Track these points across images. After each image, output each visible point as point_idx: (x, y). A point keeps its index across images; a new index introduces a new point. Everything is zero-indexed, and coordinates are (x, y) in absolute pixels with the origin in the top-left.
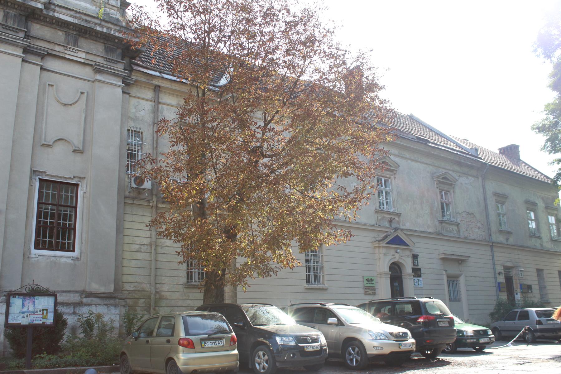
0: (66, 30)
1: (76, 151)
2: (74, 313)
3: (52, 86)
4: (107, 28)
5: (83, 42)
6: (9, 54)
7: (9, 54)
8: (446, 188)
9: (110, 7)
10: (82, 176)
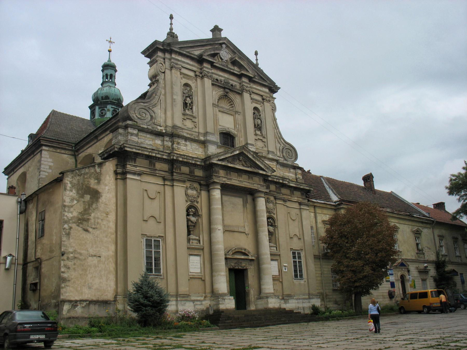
2: (309, 302)
8: (418, 236)
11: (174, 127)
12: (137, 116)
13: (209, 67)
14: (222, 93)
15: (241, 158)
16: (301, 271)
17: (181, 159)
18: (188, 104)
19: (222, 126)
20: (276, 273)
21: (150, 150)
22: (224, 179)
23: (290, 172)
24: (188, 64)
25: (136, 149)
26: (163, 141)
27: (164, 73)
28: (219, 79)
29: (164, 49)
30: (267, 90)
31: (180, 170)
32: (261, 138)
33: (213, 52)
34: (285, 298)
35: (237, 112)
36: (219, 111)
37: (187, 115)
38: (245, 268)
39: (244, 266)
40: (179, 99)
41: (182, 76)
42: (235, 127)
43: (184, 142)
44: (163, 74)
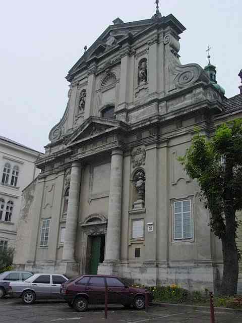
2: (188, 273)
5: (185, 123)
20: (141, 235)
36: (103, 92)
38: (102, 233)
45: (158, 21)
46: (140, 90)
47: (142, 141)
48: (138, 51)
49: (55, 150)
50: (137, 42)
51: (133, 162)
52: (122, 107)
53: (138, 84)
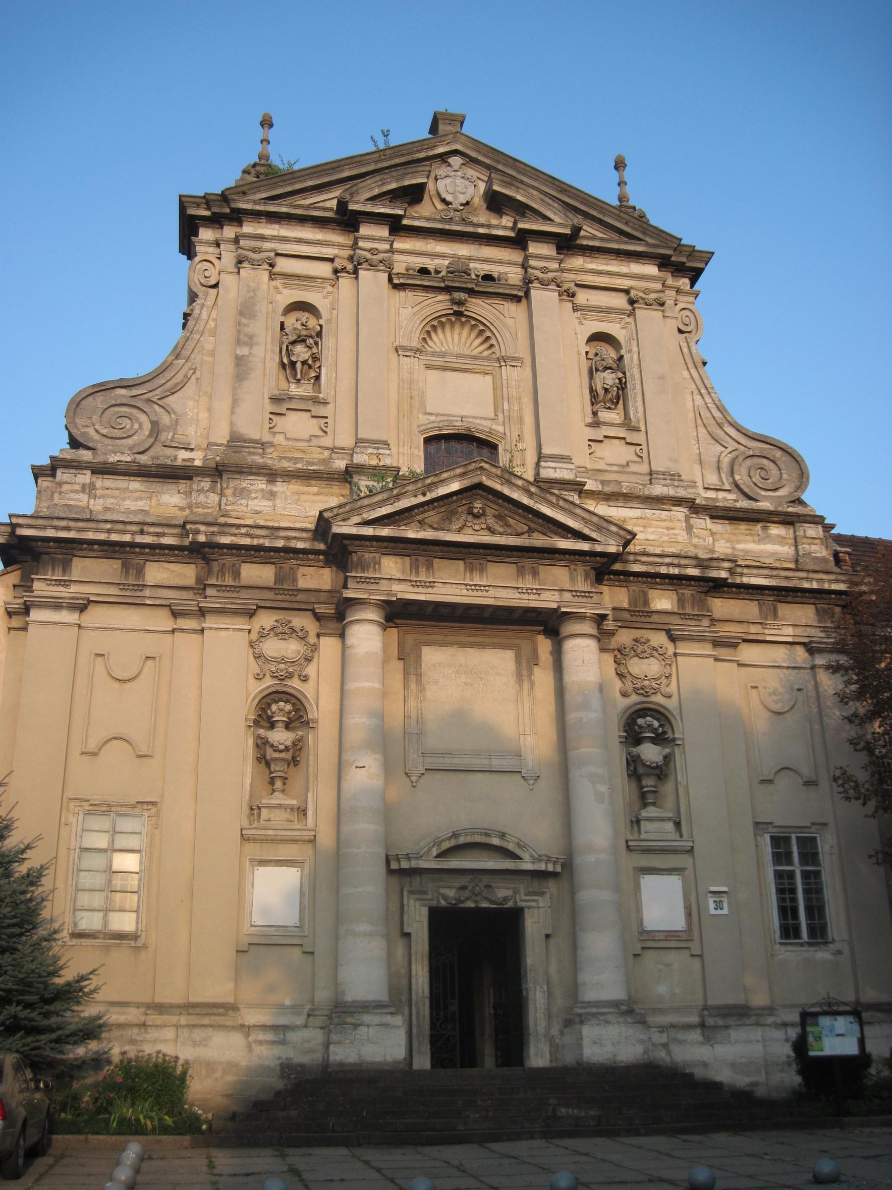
0: (759, 597)
1: (808, 783)
3: (756, 687)
4: (818, 580)
5: (784, 610)
6: (696, 655)
7: (696, 655)
9: (810, 541)
10: (823, 821)
11: (236, 441)
12: (96, 431)
13: (384, 232)
14: (440, 307)
15: (478, 505)
16: (816, 910)
17: (225, 540)
18: (299, 366)
19: (437, 415)
20: (678, 922)
21: (108, 526)
22: (396, 587)
23: (767, 539)
24: (299, 241)
25: (56, 528)
26: (188, 494)
27: (216, 286)
28: (431, 268)
29: (214, 214)
30: (652, 270)
31: (237, 574)
32: (621, 433)
33: (394, 186)
34: (710, 1021)
35: (503, 360)
36: (428, 367)
37: (291, 398)
38: (510, 904)
39: (506, 899)
40: (265, 356)
41: (278, 283)
42: (495, 410)
43: (264, 486)
44: (214, 291)
45: (675, 250)
46: (605, 437)
47: (655, 618)
48: (582, 297)
49: (132, 502)
50: (578, 262)
51: (621, 676)
52: (563, 473)
53: (595, 414)
